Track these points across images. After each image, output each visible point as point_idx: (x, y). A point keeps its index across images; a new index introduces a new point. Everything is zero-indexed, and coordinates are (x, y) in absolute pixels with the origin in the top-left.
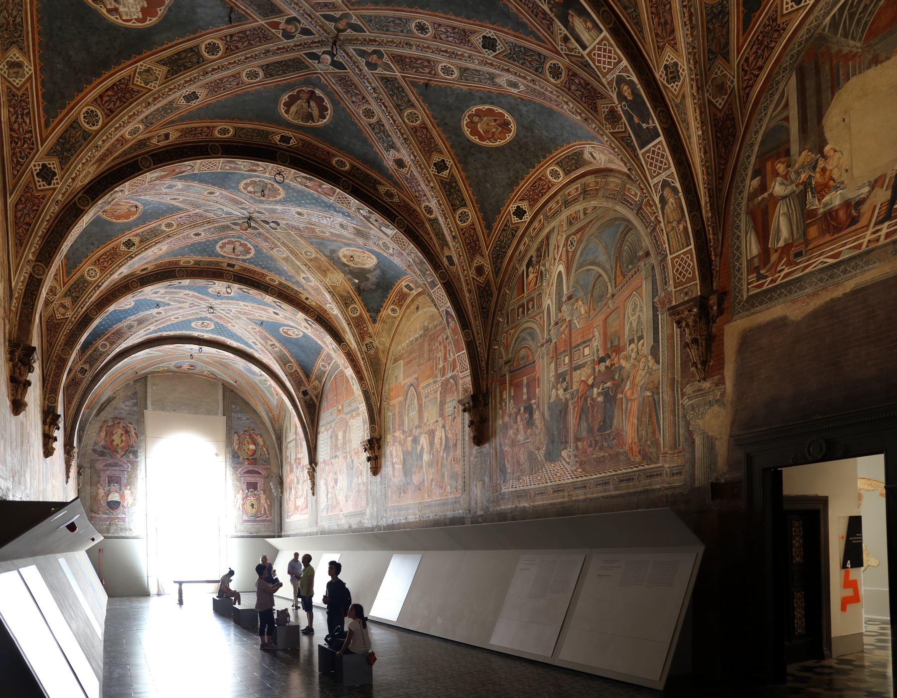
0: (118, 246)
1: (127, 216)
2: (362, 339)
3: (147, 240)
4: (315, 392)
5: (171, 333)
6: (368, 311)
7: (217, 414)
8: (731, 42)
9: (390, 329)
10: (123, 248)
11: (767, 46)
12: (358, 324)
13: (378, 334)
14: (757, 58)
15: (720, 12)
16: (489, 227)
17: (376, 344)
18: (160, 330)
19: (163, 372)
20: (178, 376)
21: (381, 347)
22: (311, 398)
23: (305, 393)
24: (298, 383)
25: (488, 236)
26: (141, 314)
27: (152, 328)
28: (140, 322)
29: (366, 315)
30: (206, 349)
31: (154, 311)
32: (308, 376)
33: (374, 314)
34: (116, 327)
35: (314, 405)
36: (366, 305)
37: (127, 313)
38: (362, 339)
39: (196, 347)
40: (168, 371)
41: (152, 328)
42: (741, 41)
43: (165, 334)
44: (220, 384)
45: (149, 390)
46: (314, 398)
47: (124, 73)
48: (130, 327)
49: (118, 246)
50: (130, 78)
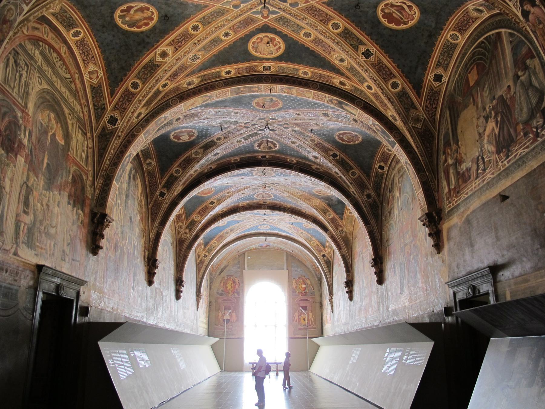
0: (207, 205)
1: (209, 193)
2: (337, 228)
3: (219, 201)
4: (330, 255)
5: (250, 232)
6: (337, 214)
7: (283, 269)
8: (415, 102)
9: (351, 222)
10: (210, 205)
11: (434, 99)
12: (333, 221)
13: (345, 225)
14: (432, 105)
15: (403, 94)
16: (368, 176)
17: (345, 230)
18: (243, 232)
19: (253, 249)
20: (261, 251)
21: (348, 232)
22: (328, 258)
23: (324, 256)
24: (320, 251)
25: (369, 180)
26: (231, 227)
27: (238, 232)
28: (231, 230)
29: (337, 217)
30: (268, 238)
31: (237, 224)
32: (324, 247)
33: (340, 216)
34: (220, 234)
35: (330, 262)
36: (335, 211)
37: (224, 227)
38: (337, 228)
39: (264, 237)
40: (256, 249)
41: (238, 232)
42: (420, 101)
43: (246, 233)
44: (285, 252)
45: (246, 260)
46: (329, 258)
47: (188, 154)
48: (227, 233)
49: (207, 205)
50: (190, 156)
